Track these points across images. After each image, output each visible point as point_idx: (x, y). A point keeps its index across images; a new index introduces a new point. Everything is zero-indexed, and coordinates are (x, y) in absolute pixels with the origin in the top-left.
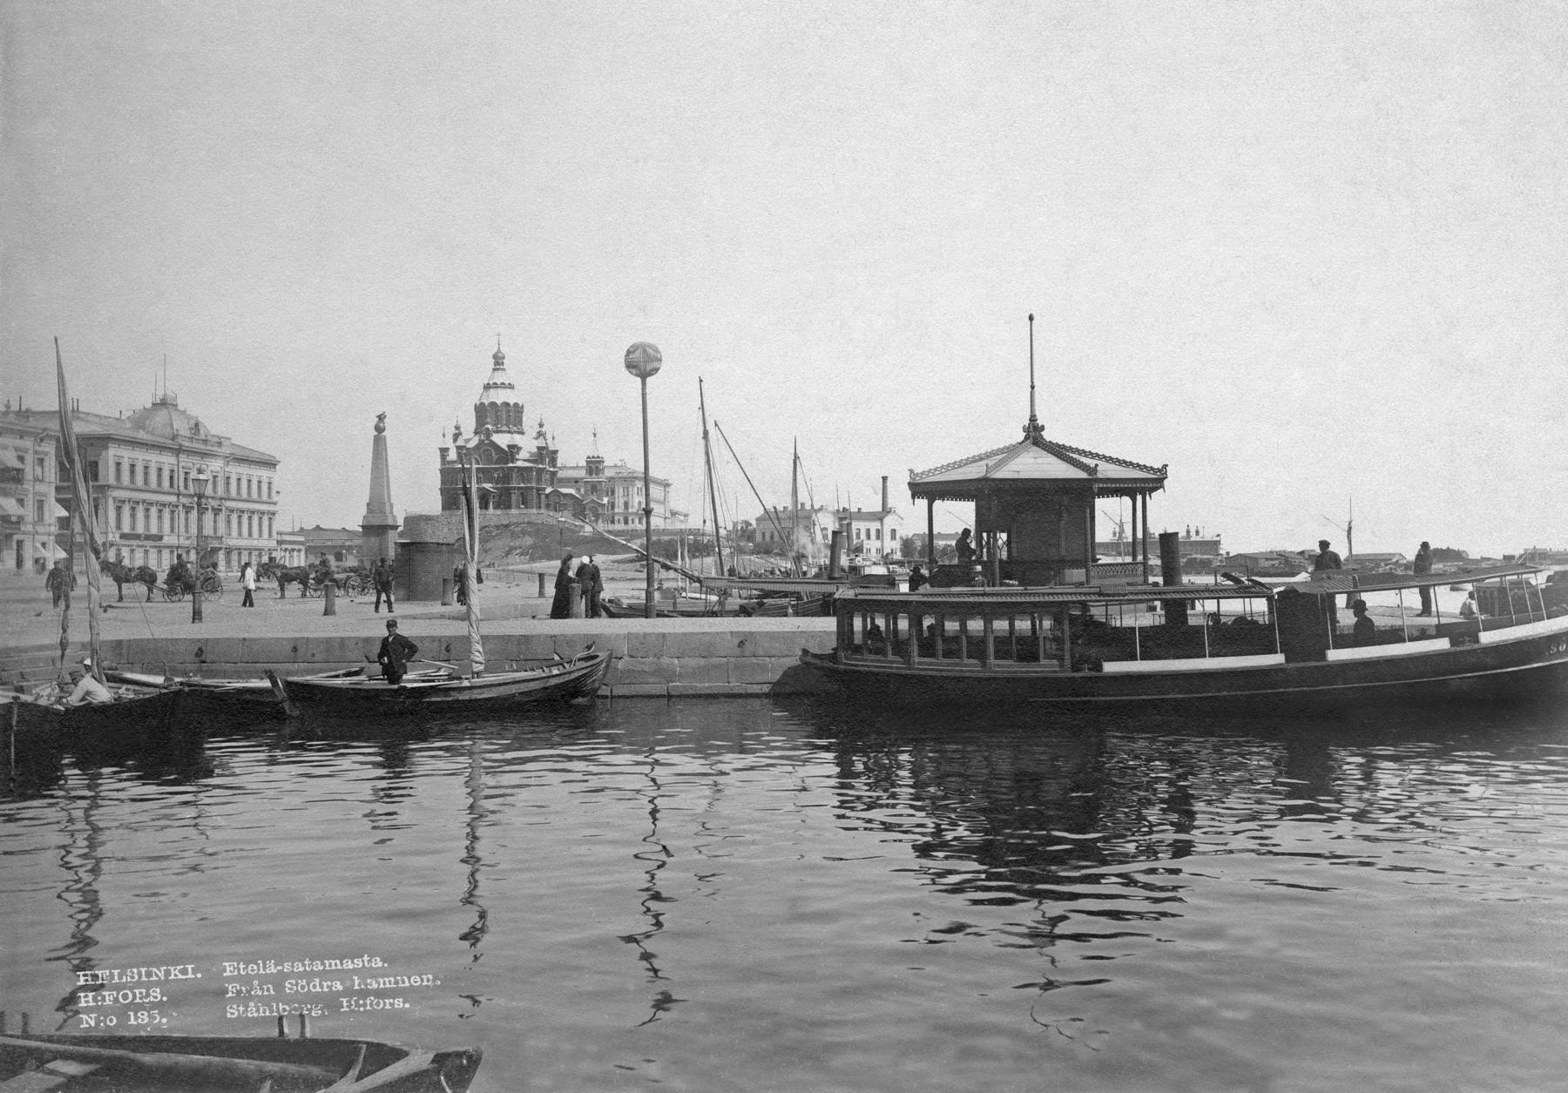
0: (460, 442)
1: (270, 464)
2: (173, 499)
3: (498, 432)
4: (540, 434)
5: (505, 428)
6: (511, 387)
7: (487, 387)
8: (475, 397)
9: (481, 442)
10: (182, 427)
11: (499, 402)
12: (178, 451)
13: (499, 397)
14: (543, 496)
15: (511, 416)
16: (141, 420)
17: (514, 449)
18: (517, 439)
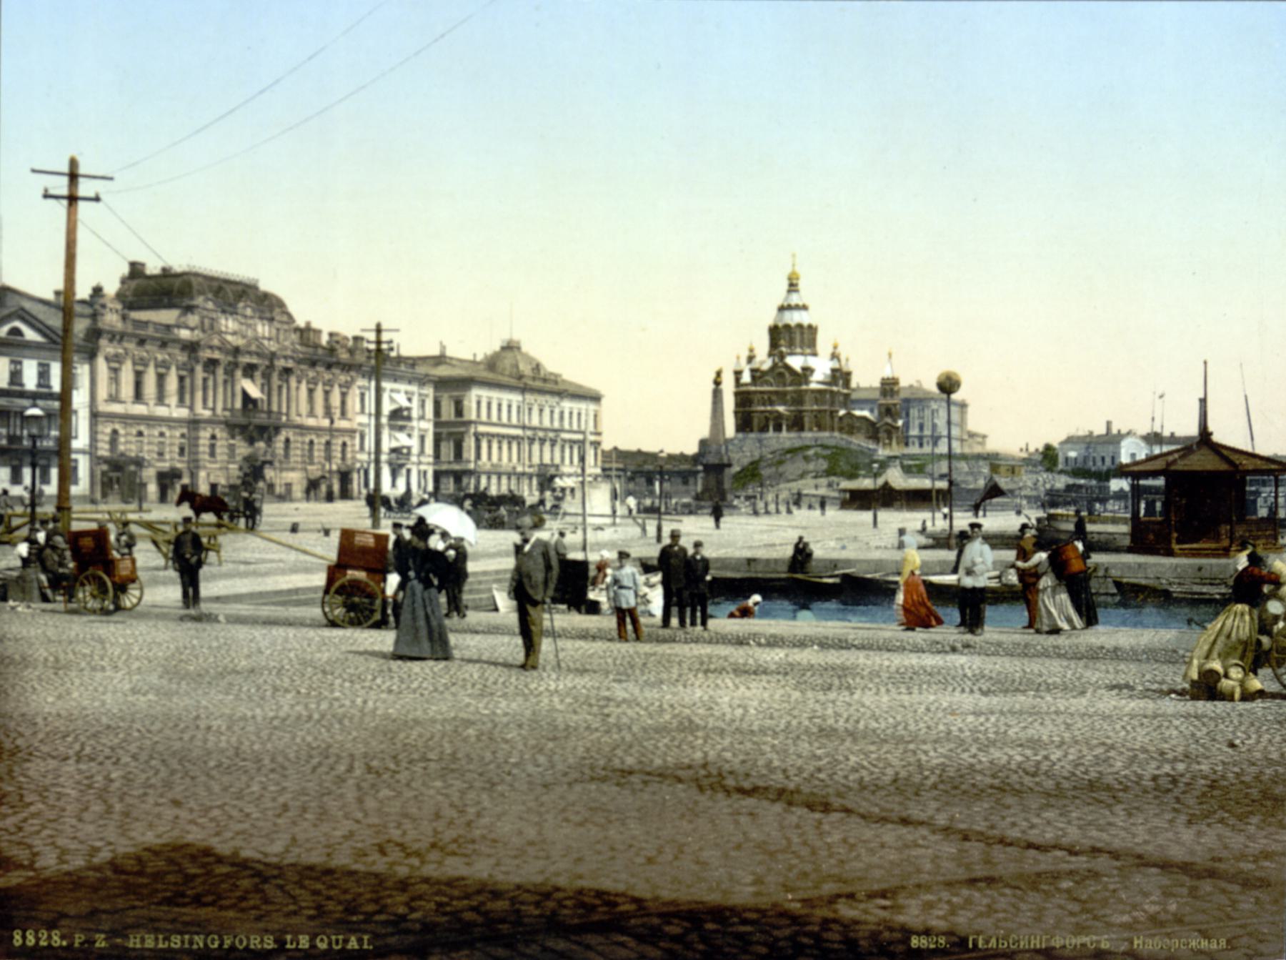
0: (755, 365)
1: (596, 398)
2: (519, 432)
3: (792, 354)
4: (834, 356)
5: (798, 350)
6: (805, 308)
7: (782, 309)
8: (769, 318)
9: (774, 366)
10: (525, 368)
11: (793, 324)
12: (524, 390)
13: (794, 318)
14: (836, 420)
15: (805, 337)
16: (492, 363)
17: (808, 371)
18: (811, 362)
